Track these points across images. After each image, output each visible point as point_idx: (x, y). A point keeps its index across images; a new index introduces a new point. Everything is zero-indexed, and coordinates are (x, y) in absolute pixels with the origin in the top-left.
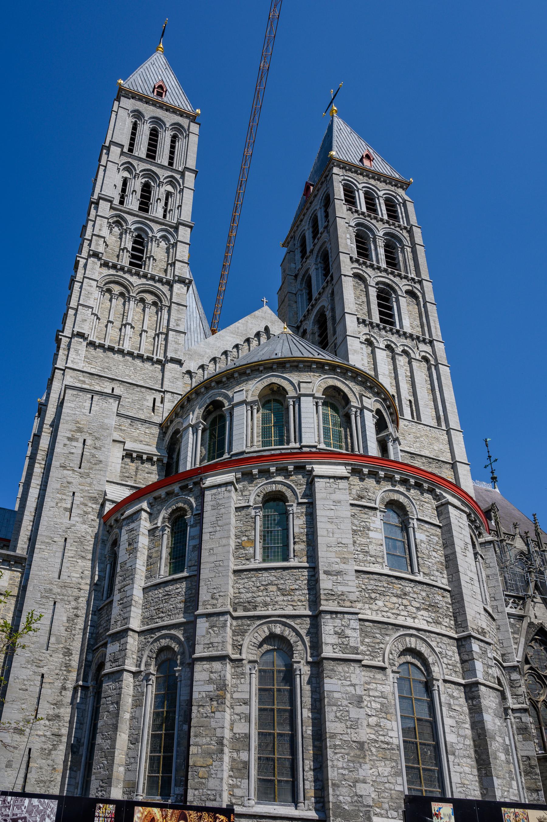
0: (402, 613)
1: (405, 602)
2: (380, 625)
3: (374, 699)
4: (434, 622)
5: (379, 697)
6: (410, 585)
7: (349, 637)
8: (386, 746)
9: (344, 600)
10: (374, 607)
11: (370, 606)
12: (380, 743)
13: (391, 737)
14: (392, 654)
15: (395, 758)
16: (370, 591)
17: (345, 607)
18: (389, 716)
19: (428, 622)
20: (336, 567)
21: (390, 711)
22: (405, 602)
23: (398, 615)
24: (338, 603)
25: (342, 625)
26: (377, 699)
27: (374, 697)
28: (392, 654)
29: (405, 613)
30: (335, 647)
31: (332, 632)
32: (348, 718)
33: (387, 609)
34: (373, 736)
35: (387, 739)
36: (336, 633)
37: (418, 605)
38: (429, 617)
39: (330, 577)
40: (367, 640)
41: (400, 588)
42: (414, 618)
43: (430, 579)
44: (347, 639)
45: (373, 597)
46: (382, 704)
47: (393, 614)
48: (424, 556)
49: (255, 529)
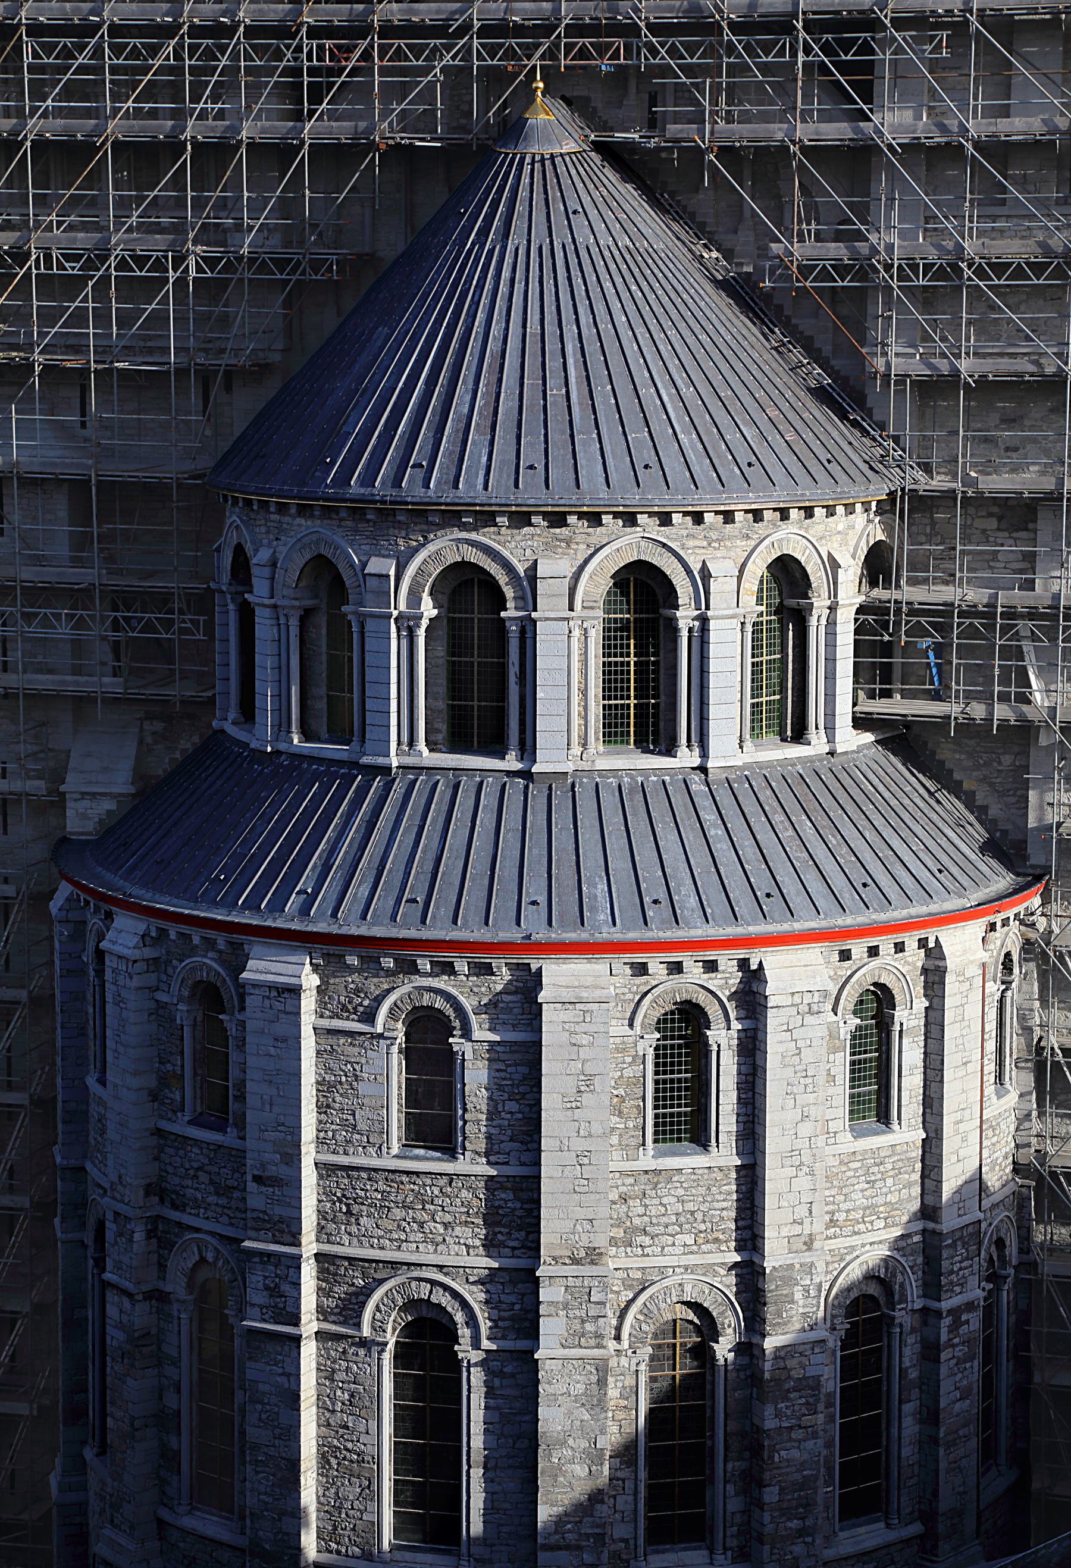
3: (340, 1384)
5: (349, 1382)
9: (283, 1232)
14: (380, 1312)
15: (367, 1475)
20: (272, 1171)
24: (274, 1235)
25: (277, 1276)
28: (380, 1312)
30: (264, 1310)
31: (260, 1286)
32: (276, 1423)
33: (381, 1233)
36: (267, 1288)
37: (448, 1218)
39: (263, 1189)
46: (352, 1396)
49: (182, 1053)
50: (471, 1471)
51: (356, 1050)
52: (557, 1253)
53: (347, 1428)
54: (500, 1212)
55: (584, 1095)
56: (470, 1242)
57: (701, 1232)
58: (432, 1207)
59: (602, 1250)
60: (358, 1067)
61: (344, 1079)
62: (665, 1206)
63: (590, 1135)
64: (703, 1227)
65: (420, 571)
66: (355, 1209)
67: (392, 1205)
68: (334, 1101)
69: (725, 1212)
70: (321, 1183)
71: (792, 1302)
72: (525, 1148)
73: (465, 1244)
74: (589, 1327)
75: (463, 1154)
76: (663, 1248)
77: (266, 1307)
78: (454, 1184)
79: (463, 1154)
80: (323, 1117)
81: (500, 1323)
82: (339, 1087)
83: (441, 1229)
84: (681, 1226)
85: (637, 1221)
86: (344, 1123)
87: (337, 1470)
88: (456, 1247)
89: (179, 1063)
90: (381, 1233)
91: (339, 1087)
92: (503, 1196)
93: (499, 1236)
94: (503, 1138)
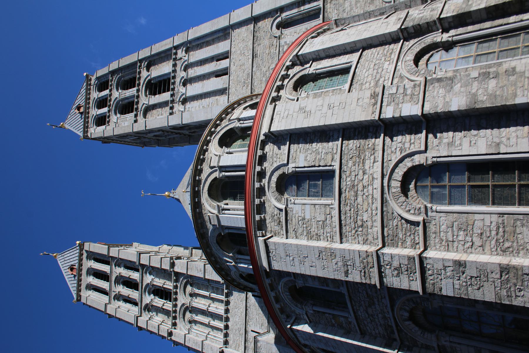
0: (371, 192)
1: (360, 187)
2: (385, 221)
3: (455, 237)
4: (374, 154)
6: (344, 180)
7: (400, 264)
8: (501, 229)
10: (369, 224)
11: (369, 227)
12: (499, 237)
13: (491, 223)
15: (512, 221)
16: (356, 226)
17: (373, 262)
18: (471, 223)
19: (374, 162)
21: (465, 220)
22: (360, 187)
23: (373, 197)
24: (371, 267)
25: (390, 268)
26: (455, 233)
27: (453, 236)
28: (410, 210)
29: (370, 188)
31: (398, 279)
33: (369, 209)
34: (493, 242)
35: (493, 226)
36: (398, 275)
37: (361, 172)
38: (370, 159)
39: (349, 272)
40: (401, 236)
41: (349, 191)
42: (373, 178)
43: (336, 153)
44: (402, 266)
45: (361, 223)
46: (460, 229)
47: (373, 204)
48: (317, 158)
50: (502, 152)
51: (294, 219)
52: (371, 112)
53: (482, 234)
54: (358, 146)
55: (306, 110)
56: (372, 161)
57: (385, 60)
58: (356, 181)
59: (373, 92)
60: (300, 218)
61: (305, 226)
62: (368, 75)
63: (322, 105)
64: (383, 59)
65: (210, 205)
66: (360, 223)
67: (356, 202)
68: (314, 231)
69: (380, 53)
70: (350, 241)
71: (422, 17)
72: (332, 137)
73: (373, 163)
74: (409, 92)
75: (333, 166)
76: (388, 72)
77: (409, 277)
78: (345, 170)
79: (333, 166)
80: (322, 238)
81: (412, 141)
82: (308, 229)
83: (366, 177)
84: (380, 67)
85: (372, 84)
86: (323, 227)
87: (513, 242)
88: (375, 167)
89: (328, 315)
90: (369, 209)
91: (308, 229)
92: (351, 146)
93: (370, 146)
94: (326, 148)
